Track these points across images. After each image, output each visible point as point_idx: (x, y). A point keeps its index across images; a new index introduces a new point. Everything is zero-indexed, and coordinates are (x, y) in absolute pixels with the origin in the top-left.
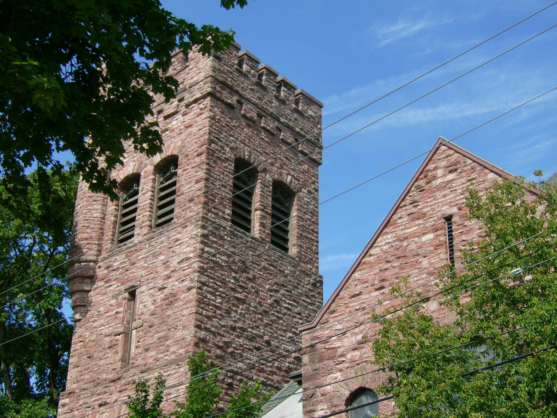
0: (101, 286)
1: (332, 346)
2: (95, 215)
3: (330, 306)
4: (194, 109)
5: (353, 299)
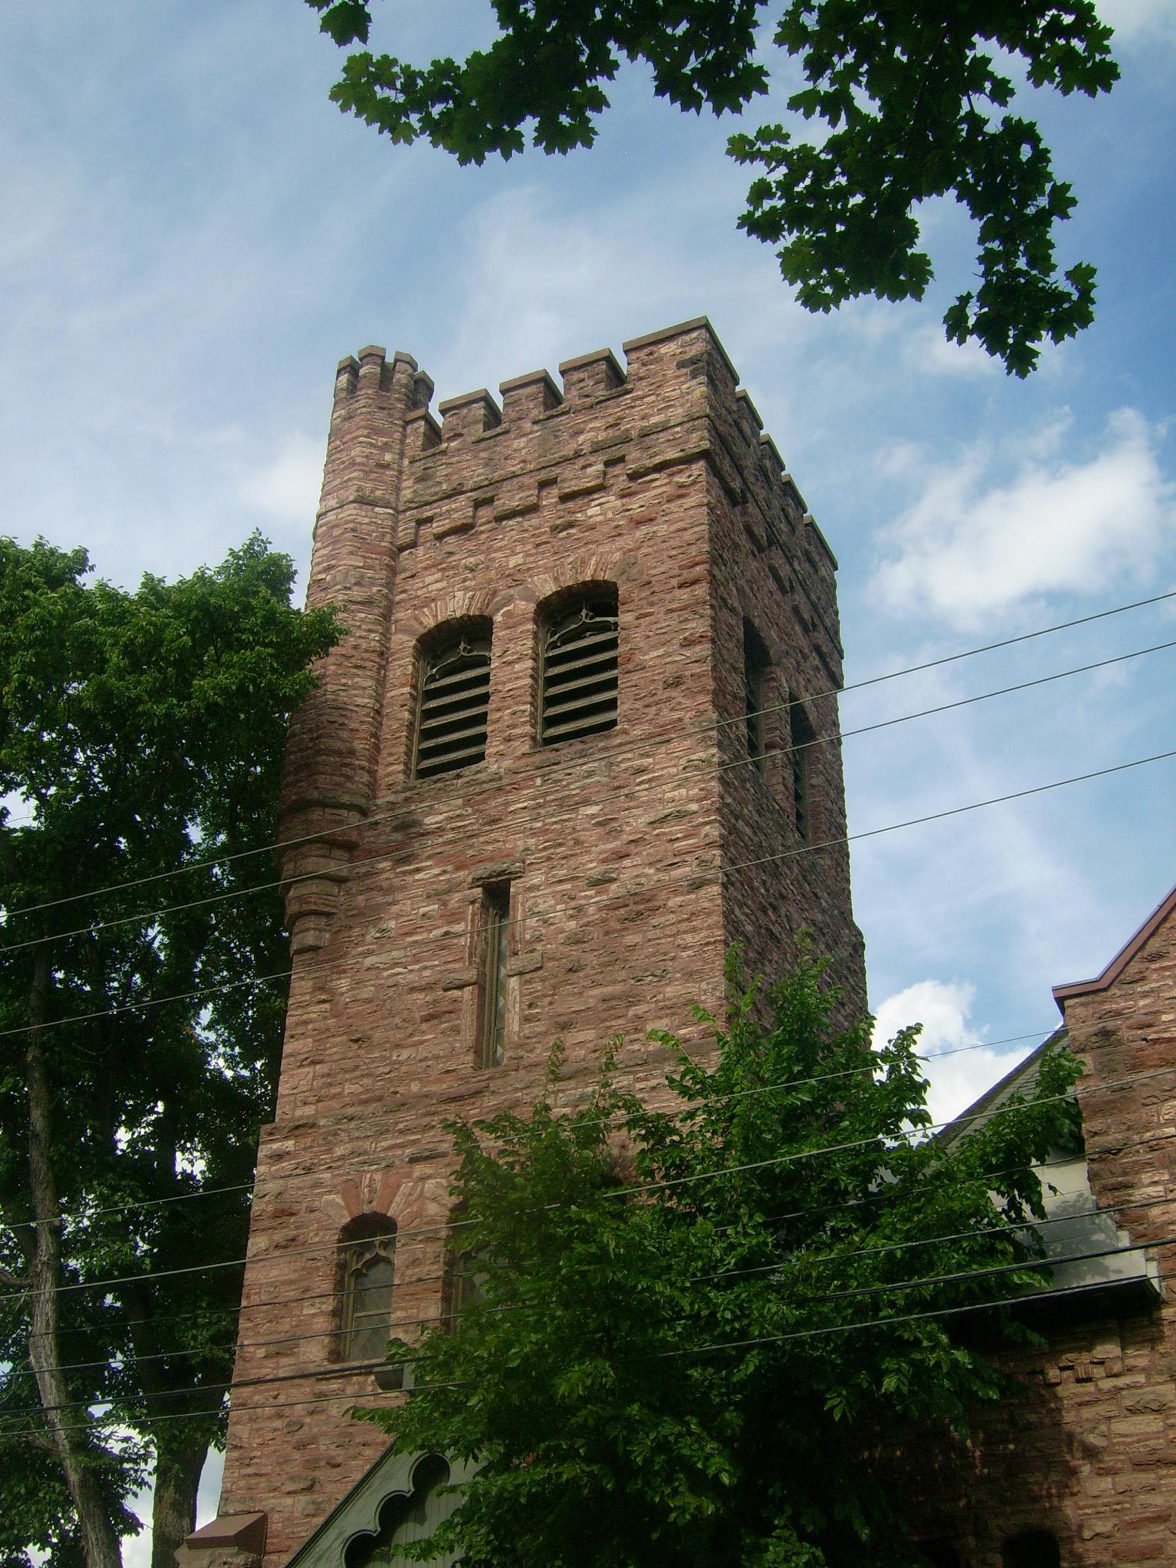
1: (1166, 1035)
2: (360, 701)
3: (1145, 943)
4: (654, 485)
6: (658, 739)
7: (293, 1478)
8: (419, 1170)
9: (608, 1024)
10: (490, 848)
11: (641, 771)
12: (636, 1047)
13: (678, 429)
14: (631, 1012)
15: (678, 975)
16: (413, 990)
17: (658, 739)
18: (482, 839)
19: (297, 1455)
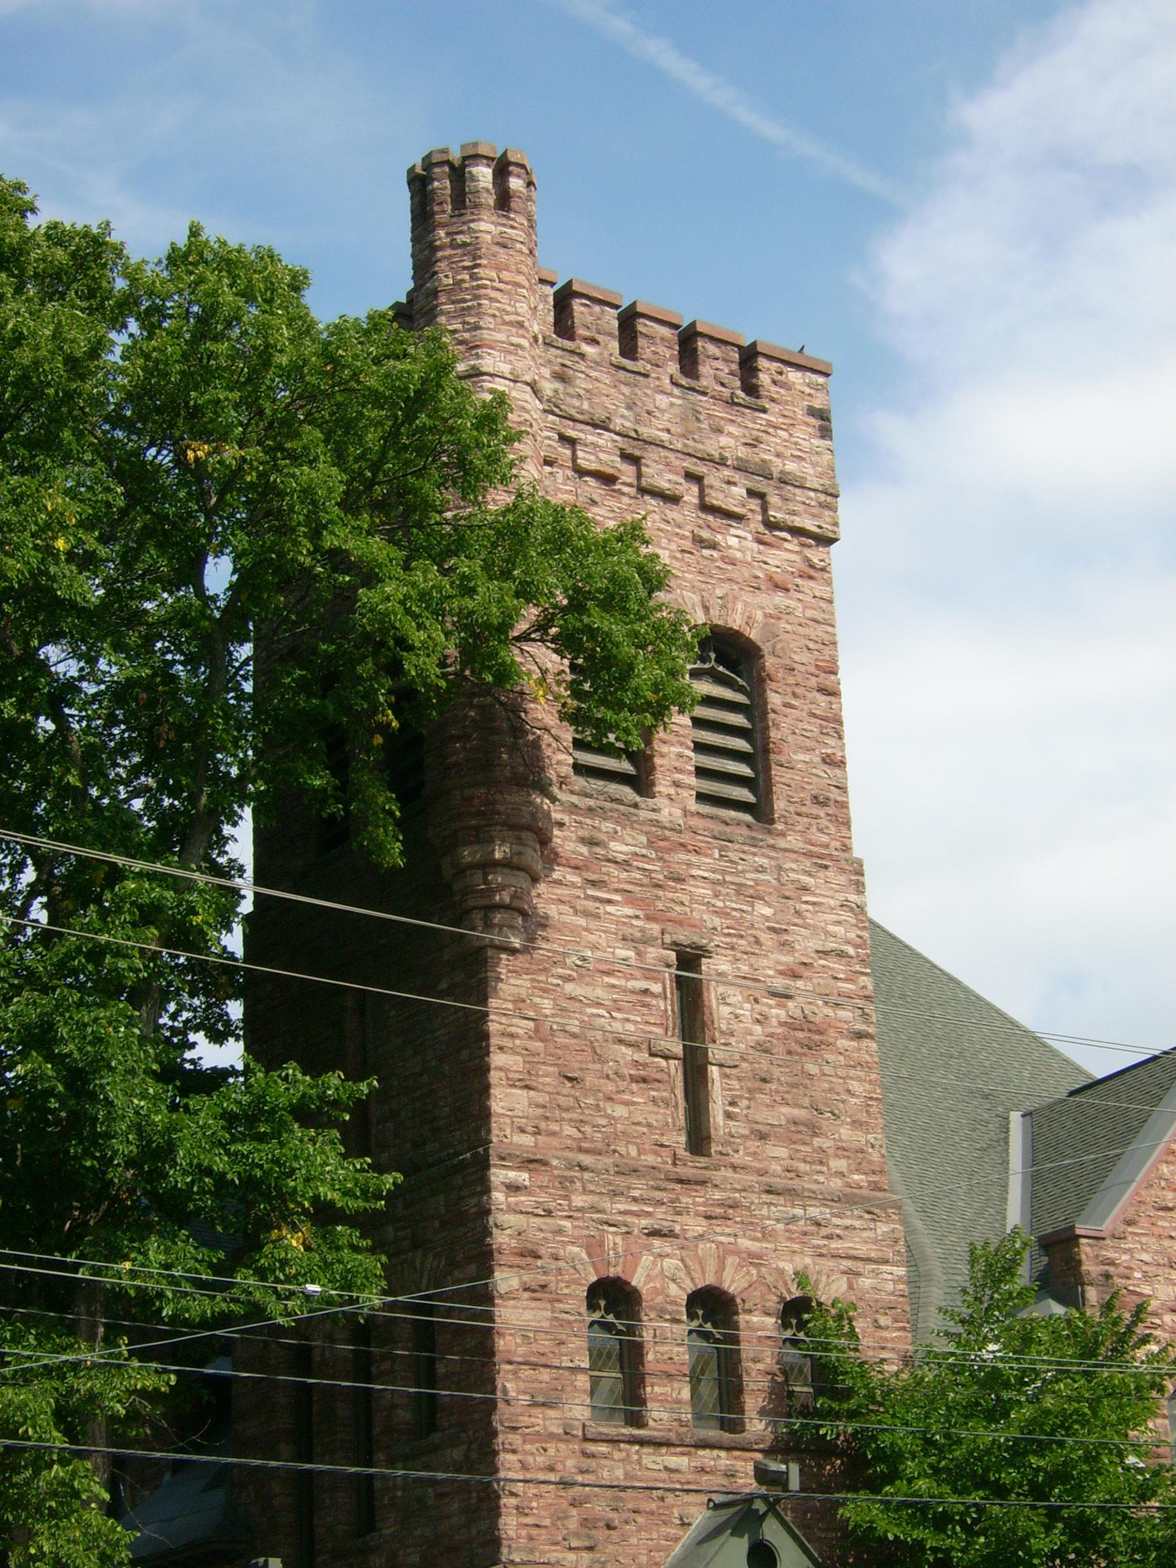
0: (573, 885)
1: (1138, 1290)
4: (787, 545)
5: (1160, 1213)
6: (819, 862)
7: (576, 1535)
8: (657, 1242)
9: (798, 1147)
10: (678, 908)
11: (805, 889)
12: (821, 1179)
13: (812, 494)
14: (817, 1142)
15: (849, 1120)
16: (621, 1041)
17: (819, 862)
18: (670, 895)
19: (574, 1512)
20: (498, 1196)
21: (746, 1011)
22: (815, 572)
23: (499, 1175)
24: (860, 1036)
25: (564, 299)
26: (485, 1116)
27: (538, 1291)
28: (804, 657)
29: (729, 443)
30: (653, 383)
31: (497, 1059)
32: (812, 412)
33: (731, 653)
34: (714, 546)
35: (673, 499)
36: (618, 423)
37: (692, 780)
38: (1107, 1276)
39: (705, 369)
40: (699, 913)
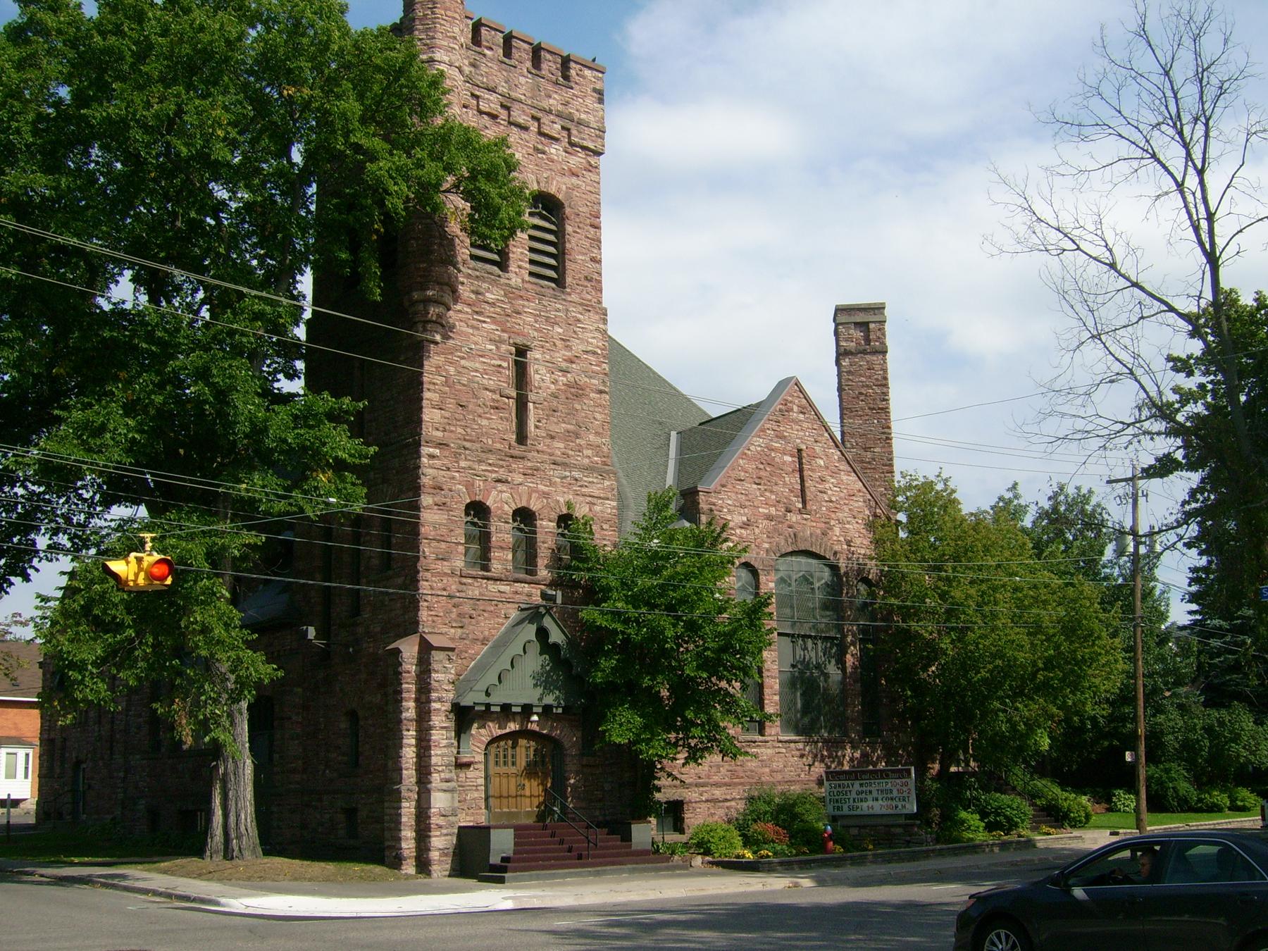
8: (500, 486)
20: (424, 460)
21: (547, 377)
22: (593, 168)
23: (425, 450)
24: (601, 392)
25: (477, 27)
26: (420, 421)
27: (441, 506)
28: (584, 209)
29: (554, 103)
30: (518, 71)
31: (426, 395)
32: (595, 90)
33: (549, 205)
34: (544, 153)
35: (525, 129)
36: (500, 89)
37: (527, 266)
38: (711, 510)
39: (544, 66)
40: (527, 329)
